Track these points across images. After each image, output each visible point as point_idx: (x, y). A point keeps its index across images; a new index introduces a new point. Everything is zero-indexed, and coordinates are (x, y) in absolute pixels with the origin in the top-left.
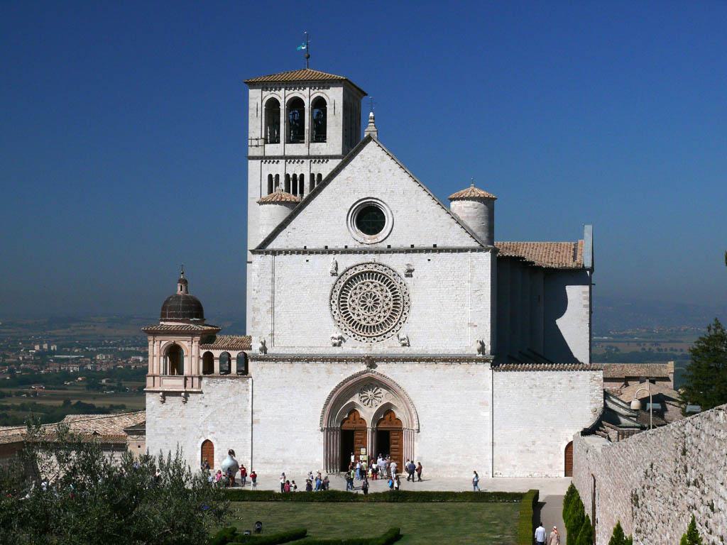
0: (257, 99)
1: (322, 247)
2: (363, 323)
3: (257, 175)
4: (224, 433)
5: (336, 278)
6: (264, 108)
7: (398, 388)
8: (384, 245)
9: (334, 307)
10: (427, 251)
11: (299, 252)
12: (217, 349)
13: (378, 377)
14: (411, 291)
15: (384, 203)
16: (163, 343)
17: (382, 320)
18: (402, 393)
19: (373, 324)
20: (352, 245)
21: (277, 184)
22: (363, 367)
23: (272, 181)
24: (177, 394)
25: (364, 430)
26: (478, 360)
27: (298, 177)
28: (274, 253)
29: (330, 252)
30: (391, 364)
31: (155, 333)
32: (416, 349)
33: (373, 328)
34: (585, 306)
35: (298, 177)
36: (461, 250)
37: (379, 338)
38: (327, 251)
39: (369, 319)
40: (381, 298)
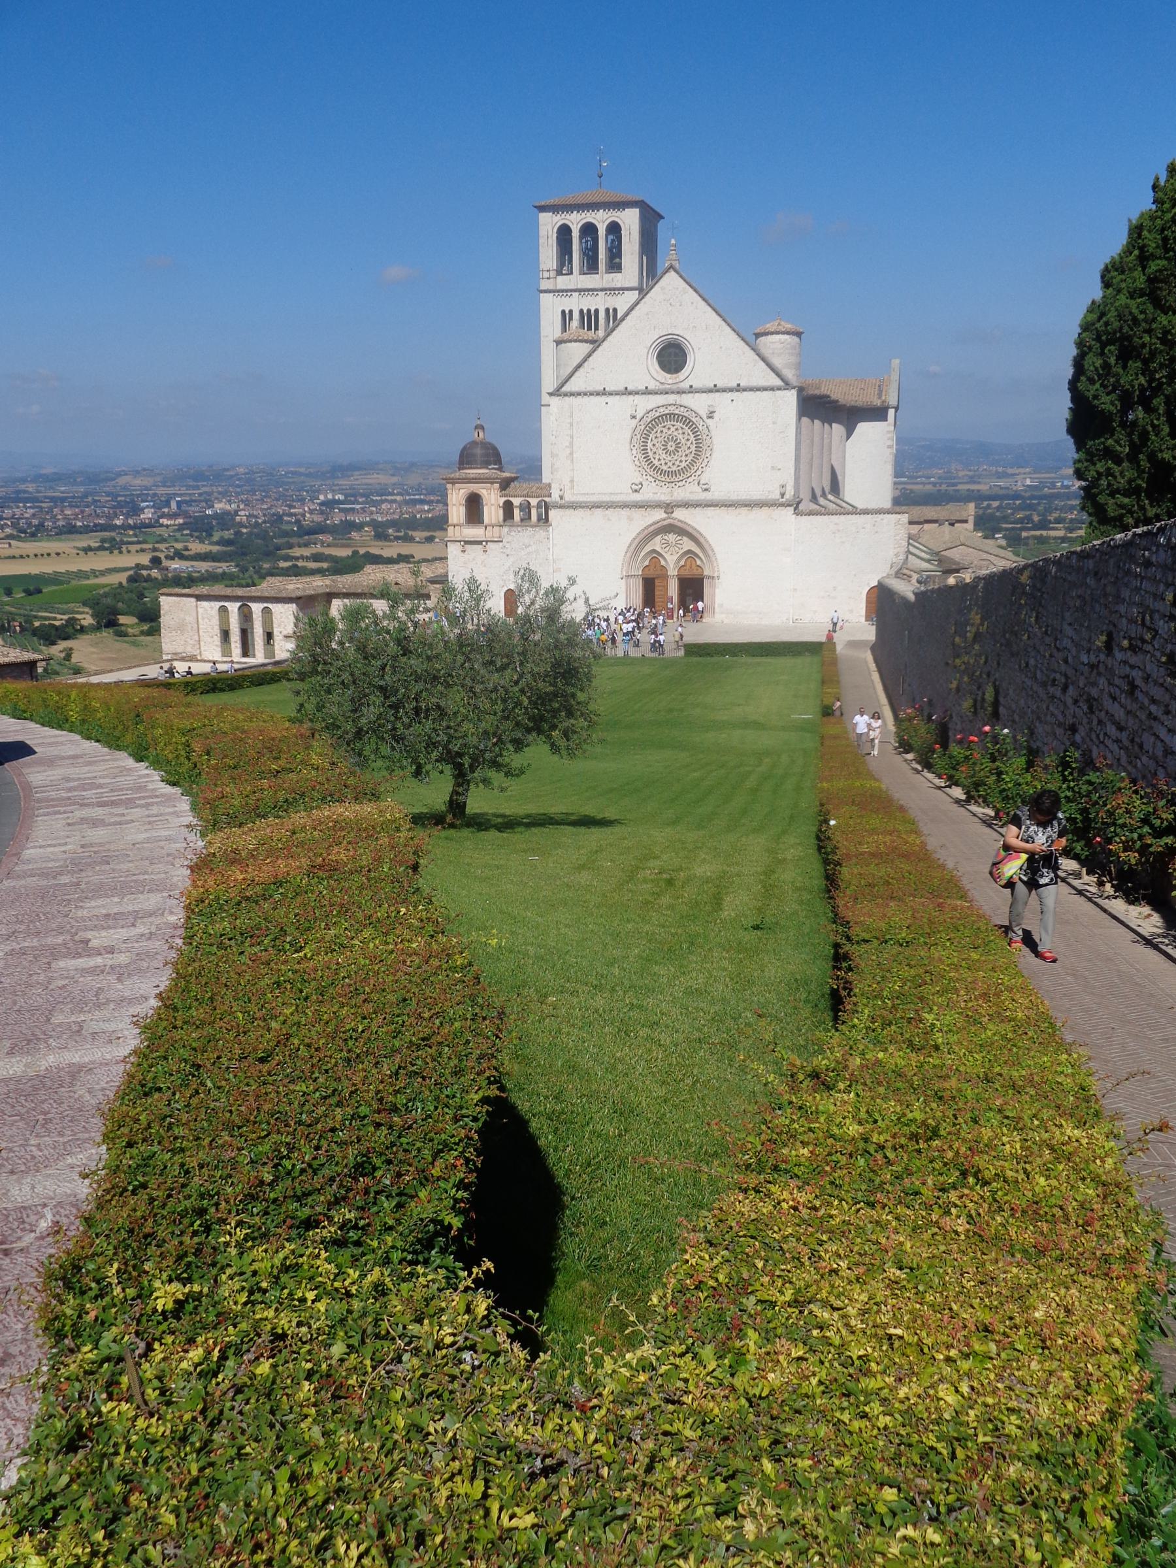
1: (621, 388)
2: (665, 468)
3: (550, 309)
5: (634, 422)
6: (555, 235)
7: (697, 536)
8: (685, 385)
9: (634, 452)
10: (731, 390)
11: (598, 394)
12: (515, 496)
14: (713, 433)
16: (462, 491)
17: (683, 465)
18: (702, 540)
19: (674, 468)
20: (653, 385)
21: (571, 318)
22: (664, 516)
23: (566, 317)
24: (480, 543)
25: (665, 577)
26: (782, 505)
28: (572, 394)
29: (630, 393)
30: (691, 510)
31: (454, 481)
32: (716, 494)
33: (675, 473)
34: (890, 447)
36: (765, 389)
37: (680, 484)
38: (626, 392)
39: (670, 464)
40: (683, 441)
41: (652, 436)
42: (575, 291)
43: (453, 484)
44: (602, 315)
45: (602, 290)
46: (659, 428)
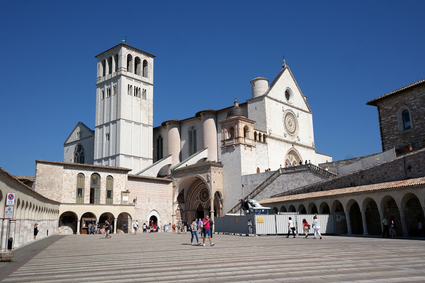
0: (125, 52)
1: (280, 100)
2: (290, 130)
3: (124, 82)
4: (262, 165)
5: (283, 112)
8: (292, 105)
13: (295, 150)
15: (291, 90)
17: (293, 131)
19: (291, 131)
20: (286, 102)
22: (292, 147)
23: (130, 87)
27: (138, 88)
35: (138, 88)
38: (280, 102)
41: (286, 119)
42: (134, 79)
43: (241, 120)
44: (142, 91)
45: (142, 82)
46: (287, 117)
